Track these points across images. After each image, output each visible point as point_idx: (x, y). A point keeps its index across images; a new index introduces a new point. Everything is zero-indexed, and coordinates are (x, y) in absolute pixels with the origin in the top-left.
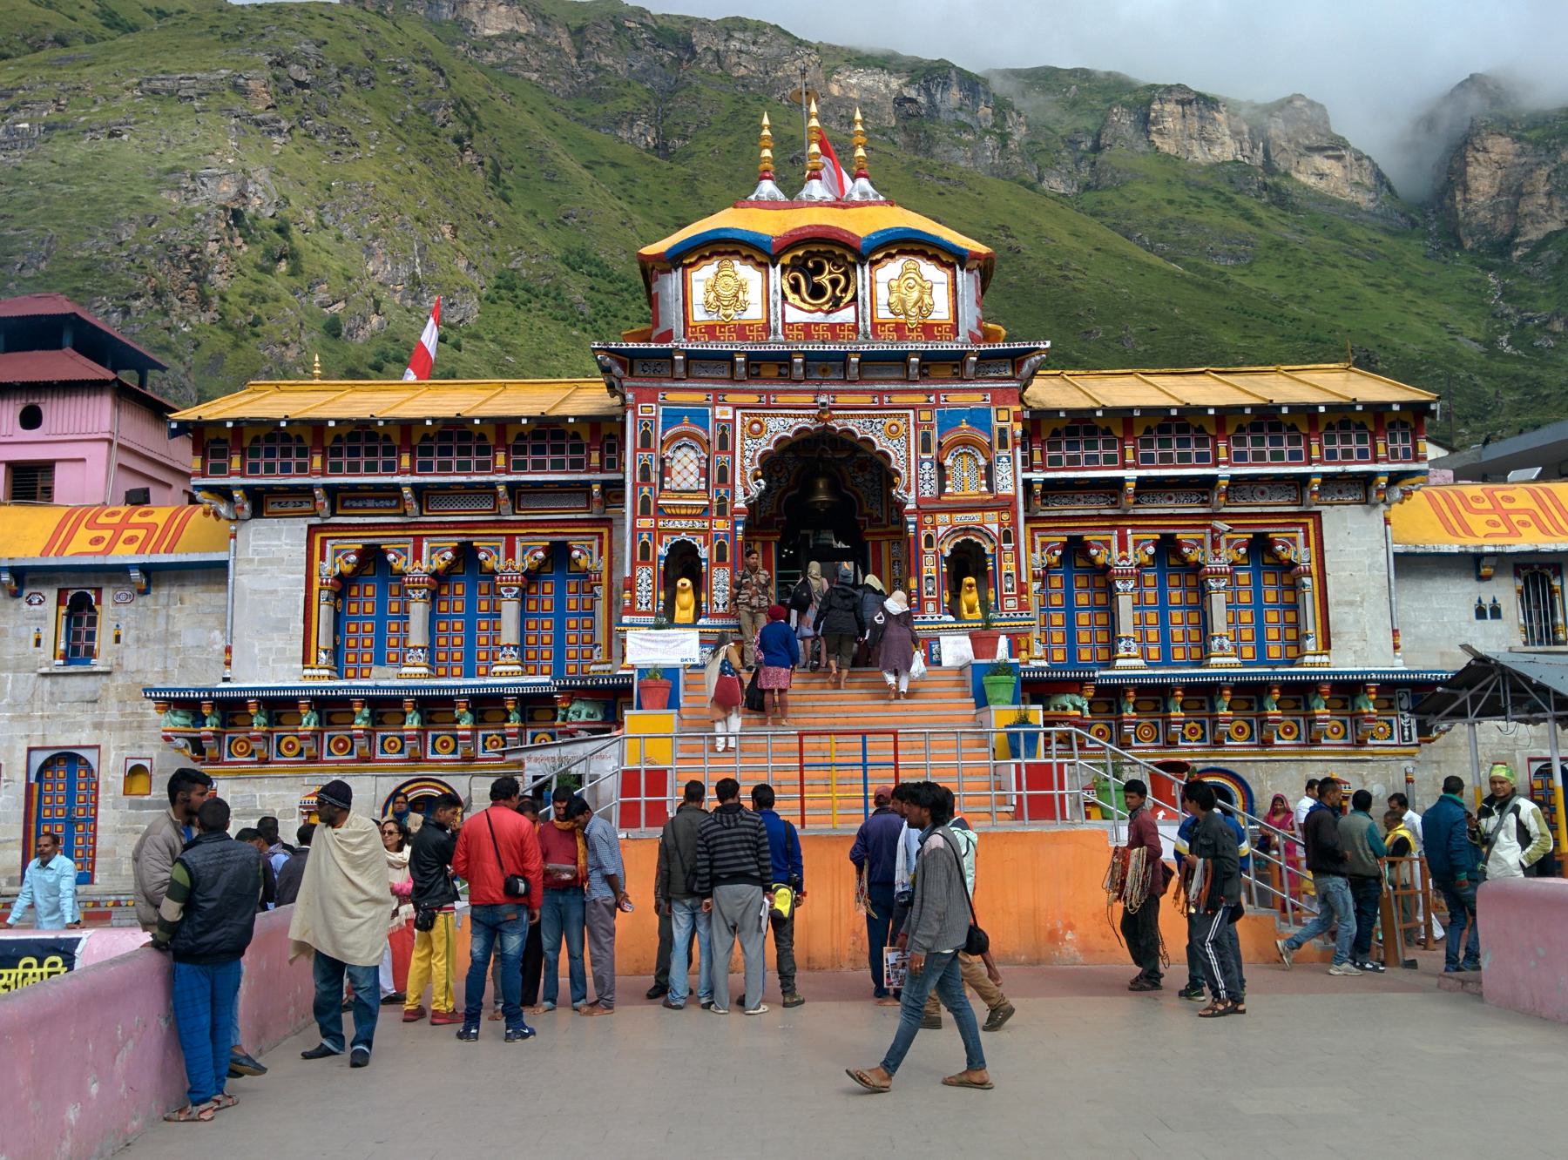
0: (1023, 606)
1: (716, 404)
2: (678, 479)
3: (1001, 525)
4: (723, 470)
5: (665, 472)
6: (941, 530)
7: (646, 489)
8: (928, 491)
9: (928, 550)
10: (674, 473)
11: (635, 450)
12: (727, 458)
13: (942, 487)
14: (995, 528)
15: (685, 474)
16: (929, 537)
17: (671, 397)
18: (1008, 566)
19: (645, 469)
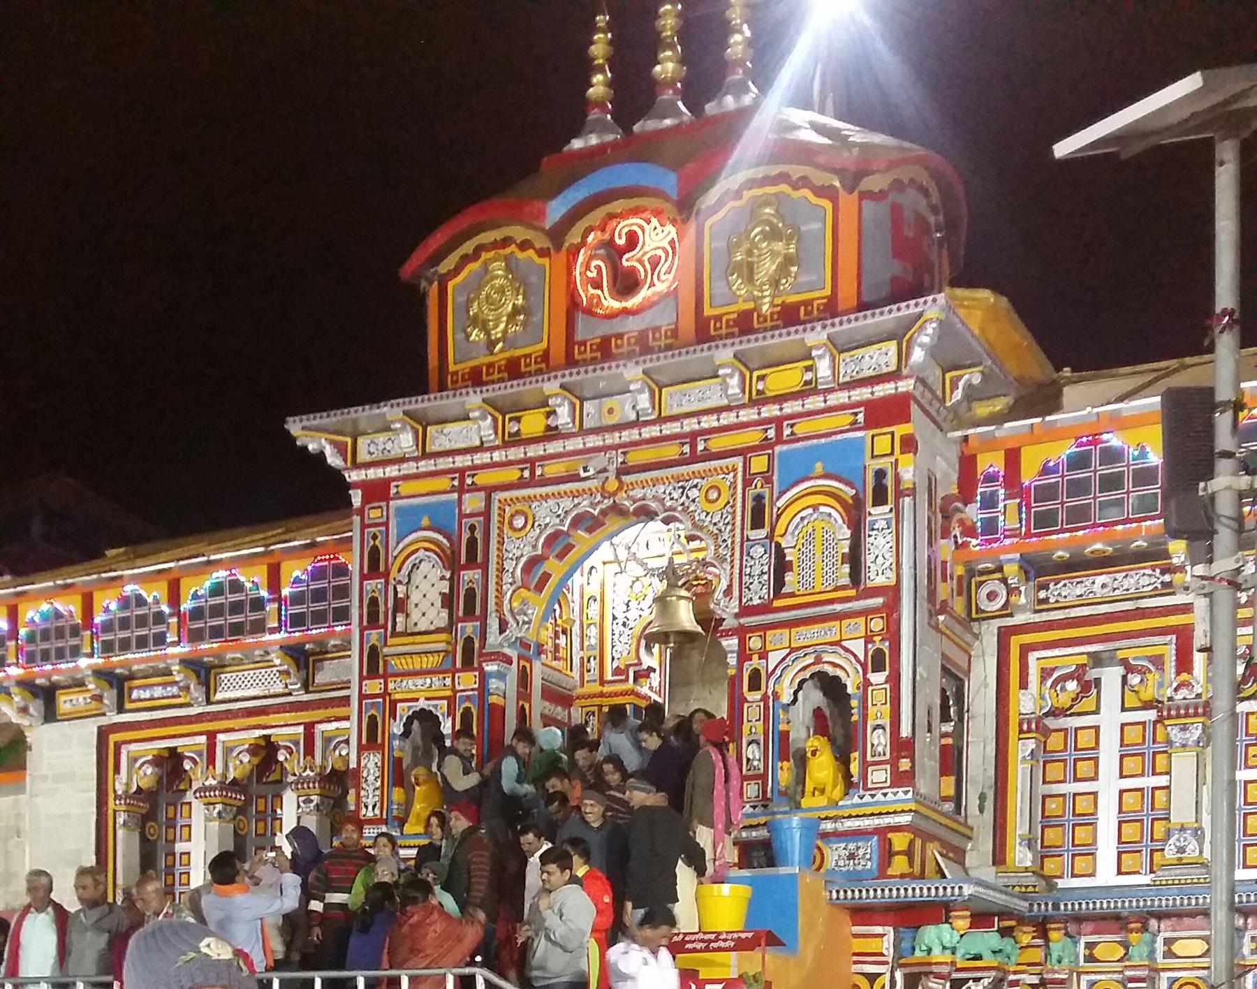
0: (901, 779)
1: (461, 490)
2: (415, 615)
3: (868, 640)
4: (471, 593)
5: (400, 605)
6: (774, 658)
7: (374, 636)
8: (758, 594)
9: (757, 696)
10: (411, 607)
11: (363, 578)
12: (476, 574)
13: (779, 582)
14: (858, 647)
15: (424, 605)
16: (755, 675)
17: (406, 488)
18: (879, 712)
19: (374, 602)
